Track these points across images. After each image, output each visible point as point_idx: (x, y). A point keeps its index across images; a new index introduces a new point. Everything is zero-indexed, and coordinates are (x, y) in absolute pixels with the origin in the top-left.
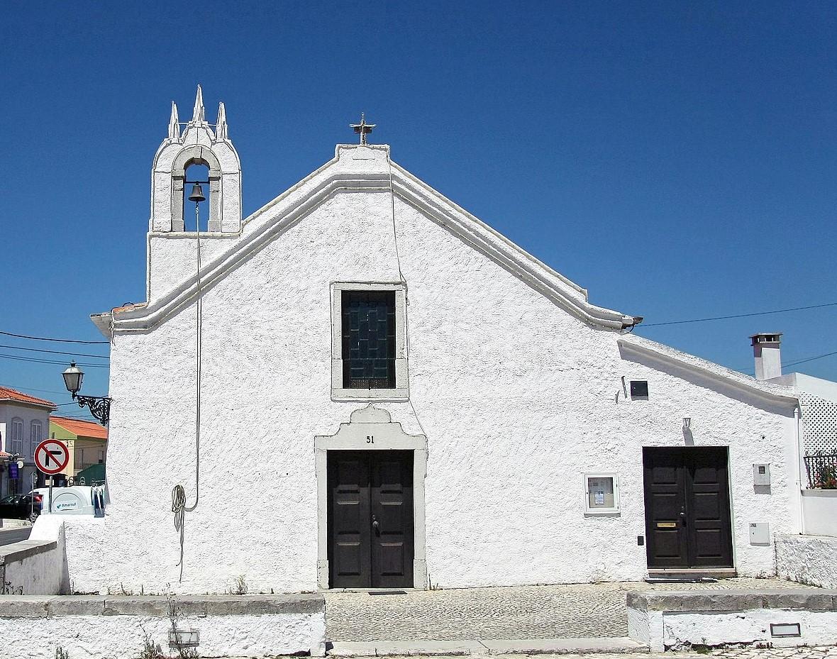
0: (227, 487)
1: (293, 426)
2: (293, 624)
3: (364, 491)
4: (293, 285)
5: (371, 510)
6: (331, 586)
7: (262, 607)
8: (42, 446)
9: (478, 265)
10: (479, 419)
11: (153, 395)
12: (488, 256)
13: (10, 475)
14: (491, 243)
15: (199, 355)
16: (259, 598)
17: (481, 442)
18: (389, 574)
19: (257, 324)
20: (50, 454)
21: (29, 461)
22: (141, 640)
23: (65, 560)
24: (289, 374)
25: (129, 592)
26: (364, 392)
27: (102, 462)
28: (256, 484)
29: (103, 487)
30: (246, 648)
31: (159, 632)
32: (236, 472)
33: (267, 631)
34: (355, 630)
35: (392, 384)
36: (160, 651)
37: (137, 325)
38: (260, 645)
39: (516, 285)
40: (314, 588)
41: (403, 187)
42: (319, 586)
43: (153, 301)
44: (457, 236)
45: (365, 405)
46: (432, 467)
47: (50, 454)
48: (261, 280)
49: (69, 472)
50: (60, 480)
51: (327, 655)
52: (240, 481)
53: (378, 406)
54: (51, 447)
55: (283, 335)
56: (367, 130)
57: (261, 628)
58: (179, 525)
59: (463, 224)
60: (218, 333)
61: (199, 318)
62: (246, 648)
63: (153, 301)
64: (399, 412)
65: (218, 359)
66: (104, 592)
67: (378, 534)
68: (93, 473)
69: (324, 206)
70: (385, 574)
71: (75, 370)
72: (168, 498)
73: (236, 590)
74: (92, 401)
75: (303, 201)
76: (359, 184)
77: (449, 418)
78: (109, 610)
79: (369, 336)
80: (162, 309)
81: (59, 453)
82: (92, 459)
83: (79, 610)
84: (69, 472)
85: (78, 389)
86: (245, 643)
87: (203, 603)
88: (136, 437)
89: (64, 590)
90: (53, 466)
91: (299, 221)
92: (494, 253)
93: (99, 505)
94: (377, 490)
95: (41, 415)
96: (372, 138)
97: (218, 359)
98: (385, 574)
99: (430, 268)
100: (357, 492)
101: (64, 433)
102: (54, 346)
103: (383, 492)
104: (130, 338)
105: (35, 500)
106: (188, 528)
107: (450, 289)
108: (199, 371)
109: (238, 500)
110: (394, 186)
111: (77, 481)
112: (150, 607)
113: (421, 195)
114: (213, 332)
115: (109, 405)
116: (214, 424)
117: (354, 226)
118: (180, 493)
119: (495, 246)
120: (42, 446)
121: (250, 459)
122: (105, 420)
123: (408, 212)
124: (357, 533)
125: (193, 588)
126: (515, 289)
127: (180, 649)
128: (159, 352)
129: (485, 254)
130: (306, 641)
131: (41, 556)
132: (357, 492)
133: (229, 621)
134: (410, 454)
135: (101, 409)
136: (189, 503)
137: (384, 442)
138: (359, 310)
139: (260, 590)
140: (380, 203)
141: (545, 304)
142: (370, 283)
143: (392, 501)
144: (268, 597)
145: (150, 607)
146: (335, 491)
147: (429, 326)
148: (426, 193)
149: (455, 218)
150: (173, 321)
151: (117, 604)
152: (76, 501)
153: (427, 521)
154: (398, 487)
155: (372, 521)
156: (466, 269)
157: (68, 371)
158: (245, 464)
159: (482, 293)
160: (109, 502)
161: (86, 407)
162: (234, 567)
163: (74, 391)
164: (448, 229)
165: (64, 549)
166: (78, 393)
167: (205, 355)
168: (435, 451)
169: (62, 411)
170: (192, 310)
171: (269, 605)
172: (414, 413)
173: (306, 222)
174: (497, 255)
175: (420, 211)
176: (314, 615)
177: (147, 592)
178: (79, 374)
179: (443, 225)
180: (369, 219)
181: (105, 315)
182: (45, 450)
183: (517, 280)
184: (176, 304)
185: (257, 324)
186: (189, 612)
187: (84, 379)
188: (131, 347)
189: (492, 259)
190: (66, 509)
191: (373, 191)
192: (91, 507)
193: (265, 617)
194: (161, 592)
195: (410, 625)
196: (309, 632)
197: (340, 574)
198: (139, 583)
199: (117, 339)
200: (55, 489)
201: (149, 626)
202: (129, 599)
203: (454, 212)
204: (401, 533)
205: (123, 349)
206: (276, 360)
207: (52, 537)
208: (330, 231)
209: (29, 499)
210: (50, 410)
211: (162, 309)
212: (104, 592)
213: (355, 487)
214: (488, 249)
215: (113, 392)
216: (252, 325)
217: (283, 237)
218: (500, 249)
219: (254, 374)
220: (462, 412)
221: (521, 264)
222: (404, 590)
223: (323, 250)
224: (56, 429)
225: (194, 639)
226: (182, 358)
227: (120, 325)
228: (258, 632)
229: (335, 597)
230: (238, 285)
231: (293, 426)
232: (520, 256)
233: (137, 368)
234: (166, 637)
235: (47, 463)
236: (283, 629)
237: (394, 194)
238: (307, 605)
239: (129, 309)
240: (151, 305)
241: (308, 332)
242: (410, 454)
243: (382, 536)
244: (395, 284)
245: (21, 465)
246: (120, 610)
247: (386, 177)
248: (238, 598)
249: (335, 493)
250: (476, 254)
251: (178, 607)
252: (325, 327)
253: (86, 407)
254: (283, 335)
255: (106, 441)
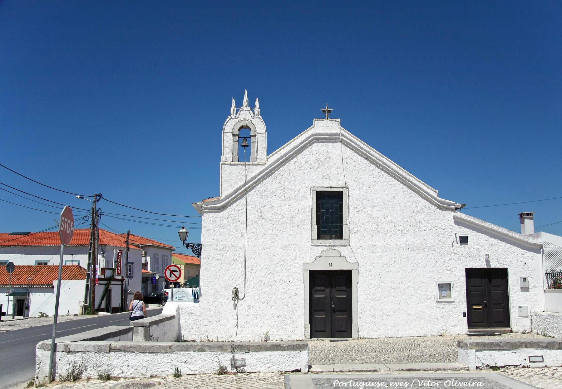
0: (260, 288)
1: (292, 258)
2: (292, 356)
3: (328, 290)
4: (292, 188)
5: (331, 300)
6: (311, 337)
7: (277, 347)
8: (168, 268)
9: (384, 178)
10: (384, 254)
11: (223, 243)
12: (389, 174)
13: (152, 282)
14: (390, 167)
15: (246, 222)
16: (274, 343)
17: (385, 266)
18: (340, 331)
19: (274, 208)
20: (172, 272)
21: (161, 275)
22: (217, 364)
23: (179, 324)
24: (290, 232)
25: (211, 340)
26: (327, 241)
27: (198, 276)
28: (274, 287)
29: (198, 288)
30: (269, 368)
31: (226, 359)
32: (264, 281)
33: (279, 360)
34: (323, 359)
35: (341, 237)
36: (226, 369)
37: (215, 208)
38: (276, 366)
39: (403, 188)
40: (302, 338)
41: (346, 140)
42: (305, 337)
43: (223, 196)
44: (373, 164)
45: (328, 248)
46: (361, 278)
47: (172, 272)
48: (277, 186)
49: (182, 281)
50: (177, 285)
51: (309, 371)
52: (266, 285)
53: (334, 248)
54: (173, 268)
55: (287, 213)
56: (329, 112)
57: (277, 358)
58: (236, 307)
59: (377, 158)
60: (255, 212)
61: (246, 205)
62: (269, 368)
63: (223, 196)
64: (344, 251)
65: (255, 225)
66: (198, 340)
67: (334, 311)
68: (193, 281)
69: (307, 149)
70: (338, 331)
71: (184, 230)
72: (231, 293)
73: (264, 339)
74: (192, 246)
75: (297, 147)
76: (325, 139)
77: (370, 254)
78: (201, 349)
79: (330, 213)
80: (227, 200)
81: (177, 271)
82: (193, 274)
83: (186, 349)
84: (182, 281)
85: (186, 240)
86: (268, 365)
87: (247, 346)
88: (215, 264)
89: (179, 339)
90: (173, 278)
91: (295, 157)
92: (392, 172)
93: (196, 297)
94: (334, 290)
95: (167, 252)
96: (331, 115)
97: (255, 225)
98: (338, 331)
99: (360, 180)
100: (324, 291)
101: (179, 261)
102: (174, 218)
103: (337, 291)
104: (211, 214)
105: (165, 295)
106: (240, 308)
107: (370, 190)
108: (246, 231)
109: (265, 295)
110: (342, 139)
111: (185, 285)
112: (221, 347)
113: (356, 144)
114: (253, 211)
115: (201, 248)
116: (254, 257)
117: (322, 160)
118: (236, 291)
119: (392, 169)
120: (168, 268)
121: (271, 275)
122: (199, 255)
123: (348, 152)
124: (324, 311)
125: (242, 338)
126: (402, 190)
127: (236, 368)
128: (226, 221)
129: (387, 173)
130: (299, 364)
131: (167, 322)
132: (324, 291)
133: (261, 355)
134: (350, 272)
135: (197, 250)
136: (241, 296)
137: (336, 267)
138: (325, 201)
139: (276, 339)
140: (335, 148)
141: (417, 197)
142: (330, 187)
143: (341, 295)
144: (280, 342)
145: (221, 347)
146: (313, 290)
147: (360, 209)
148: (358, 143)
149: (372, 155)
150: (233, 206)
151: (205, 346)
152: (185, 295)
153: (359, 305)
154: (344, 288)
155: (331, 305)
156: (378, 180)
157: (181, 231)
158: (269, 277)
159: (386, 193)
160: (201, 295)
161: (190, 249)
162: (263, 328)
163: (184, 241)
164: (369, 160)
165: (179, 319)
166: (186, 242)
167: (249, 223)
168: (362, 270)
169: (178, 250)
170: (242, 200)
171: (281, 347)
172: (352, 252)
173: (298, 157)
174: (394, 174)
175: (355, 152)
176: (303, 352)
177: (220, 340)
178: (186, 232)
179: (367, 159)
180: (330, 155)
181: (199, 203)
182: (170, 270)
183: (403, 186)
184: (234, 198)
185: (274, 208)
186: (241, 350)
187: (189, 235)
188: (212, 219)
189: (391, 176)
190: (180, 299)
191: (332, 142)
192: (192, 298)
193: (279, 352)
194: (227, 340)
195: (351, 356)
196: (300, 359)
197: (316, 331)
198: (216, 335)
199: (205, 215)
200: (174, 289)
201: (221, 357)
202: (211, 344)
203: (372, 152)
204: (346, 311)
205: (208, 219)
206: (284, 225)
207: (173, 313)
208: (311, 161)
209: (161, 294)
210: (172, 250)
211: (227, 200)
212: (198, 340)
213: (323, 288)
214: (389, 170)
215: (203, 241)
216: (272, 208)
217: (287, 164)
218: (395, 171)
219: (273, 232)
220: (376, 251)
221: (405, 178)
222: (348, 339)
223: (307, 171)
224: (175, 259)
225: (243, 363)
226: (237, 224)
227: (207, 208)
228: (275, 360)
229: (314, 343)
230: (265, 188)
231: (292, 258)
232: (405, 174)
233: (215, 229)
234: (229, 362)
235: (171, 276)
236: (287, 358)
237: (342, 143)
238: (299, 346)
239: (211, 200)
240: (222, 198)
241: (300, 211)
242: (350, 272)
243: (337, 313)
244: (343, 188)
245: (157, 277)
246: (206, 349)
247: (338, 135)
248: (265, 343)
249: (313, 291)
250: (383, 173)
251: (235, 348)
252: (308, 209)
253: (190, 249)
254: (287, 213)
255: (199, 265)
